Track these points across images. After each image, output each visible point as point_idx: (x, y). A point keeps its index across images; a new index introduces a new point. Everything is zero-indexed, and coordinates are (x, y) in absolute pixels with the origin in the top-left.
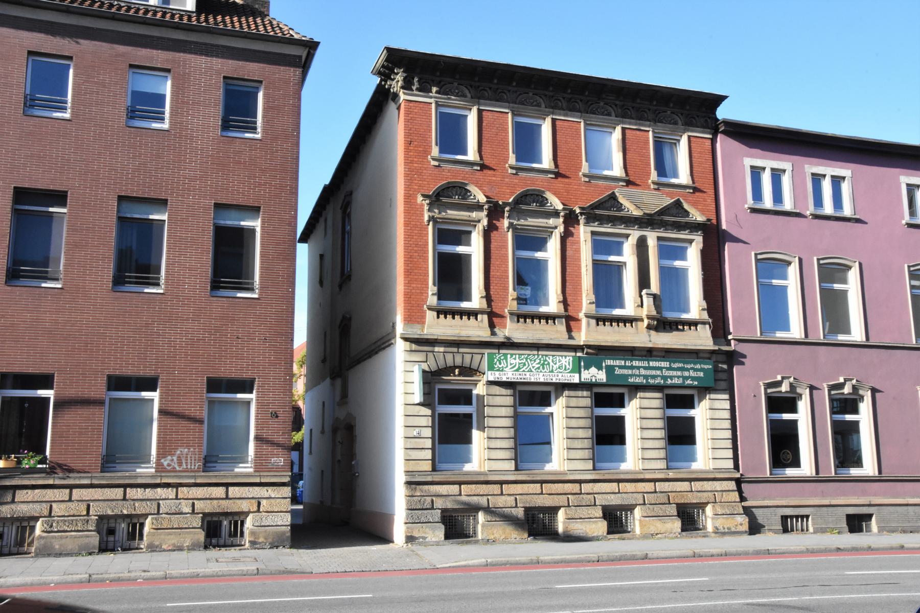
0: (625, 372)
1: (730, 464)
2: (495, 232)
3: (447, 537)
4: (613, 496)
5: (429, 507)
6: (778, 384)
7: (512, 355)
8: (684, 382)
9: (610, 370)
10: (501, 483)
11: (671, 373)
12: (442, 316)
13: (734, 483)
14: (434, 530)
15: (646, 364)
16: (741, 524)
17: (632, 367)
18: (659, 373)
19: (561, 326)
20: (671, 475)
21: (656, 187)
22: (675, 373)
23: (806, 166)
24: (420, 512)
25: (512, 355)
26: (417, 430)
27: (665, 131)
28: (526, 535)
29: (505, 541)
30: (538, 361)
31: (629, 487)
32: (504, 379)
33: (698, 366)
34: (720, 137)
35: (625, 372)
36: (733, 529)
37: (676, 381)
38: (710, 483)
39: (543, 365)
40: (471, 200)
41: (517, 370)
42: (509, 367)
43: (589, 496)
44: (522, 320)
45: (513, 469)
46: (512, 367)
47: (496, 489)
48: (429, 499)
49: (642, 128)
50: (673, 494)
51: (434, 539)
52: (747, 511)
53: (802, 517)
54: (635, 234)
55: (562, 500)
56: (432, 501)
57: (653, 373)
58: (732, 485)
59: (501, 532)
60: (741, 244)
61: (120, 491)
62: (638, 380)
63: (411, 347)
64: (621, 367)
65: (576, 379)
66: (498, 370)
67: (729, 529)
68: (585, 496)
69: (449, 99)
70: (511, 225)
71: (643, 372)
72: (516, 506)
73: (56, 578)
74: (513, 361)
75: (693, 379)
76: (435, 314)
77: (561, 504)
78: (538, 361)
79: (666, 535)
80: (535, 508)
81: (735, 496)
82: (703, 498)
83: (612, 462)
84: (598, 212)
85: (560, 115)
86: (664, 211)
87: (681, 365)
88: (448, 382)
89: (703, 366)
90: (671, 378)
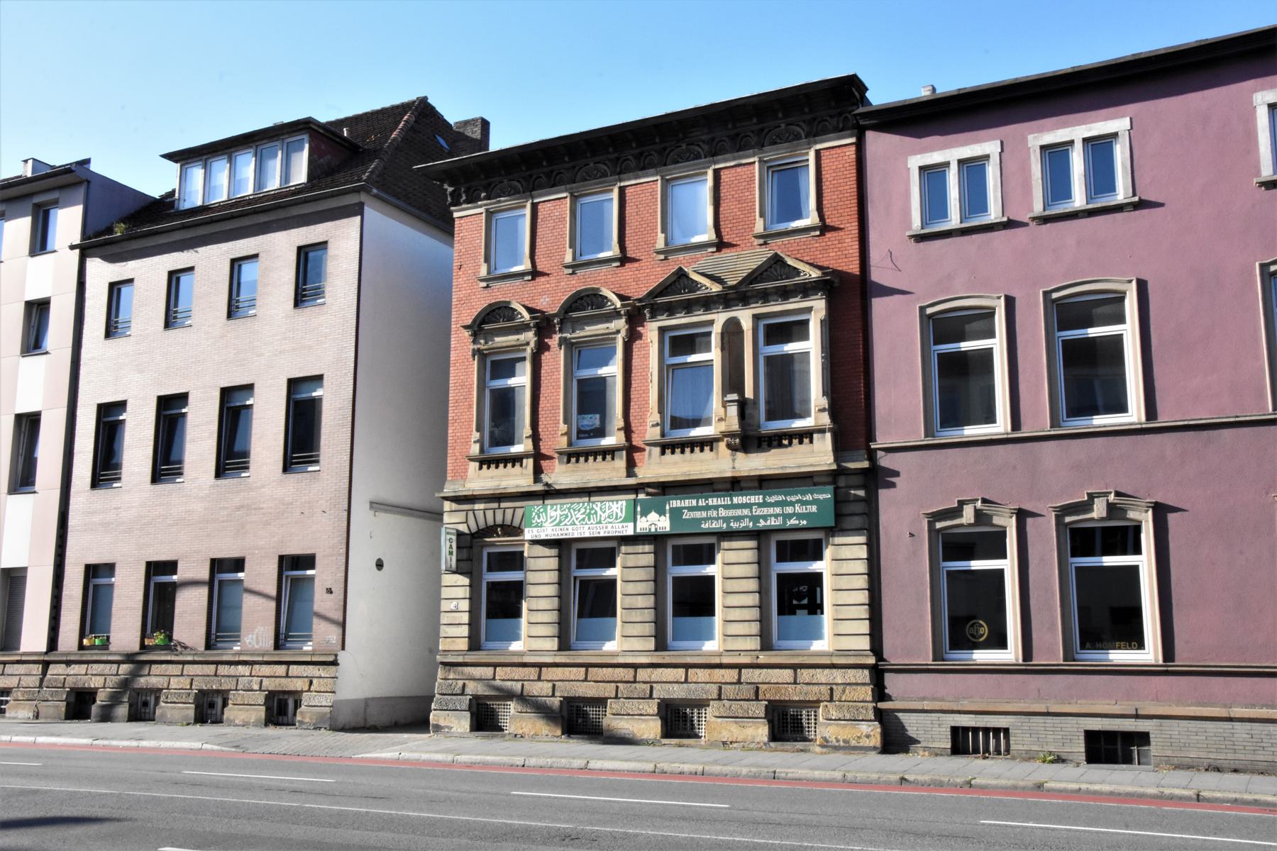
0: (698, 514)
1: (864, 644)
3: (775, 736)
4: (676, 686)
6: (956, 512)
8: (785, 522)
9: (676, 514)
10: (540, 666)
11: (765, 511)
13: (866, 672)
14: (459, 719)
15: (727, 501)
16: (868, 736)
17: (707, 508)
18: (746, 512)
19: (620, 463)
20: (763, 658)
21: (761, 241)
22: (771, 511)
23: (1030, 137)
25: (552, 505)
26: (455, 602)
27: (776, 154)
28: (559, 732)
31: (702, 675)
32: (543, 537)
33: (809, 497)
34: (870, 136)
35: (698, 514)
36: (853, 743)
37: (773, 523)
38: (827, 671)
40: (609, 308)
41: (558, 525)
43: (644, 686)
44: (573, 460)
45: (556, 648)
46: (550, 521)
47: (532, 673)
48: (460, 683)
52: (880, 716)
53: (997, 731)
54: (720, 318)
55: (608, 690)
56: (464, 685)
57: (739, 512)
58: (864, 675)
61: (681, 671)
62: (716, 526)
64: (691, 509)
65: (629, 531)
67: (844, 741)
70: (563, 341)
71: (723, 513)
72: (553, 695)
73: (745, 771)
74: (553, 514)
76: (477, 464)
77: (607, 695)
79: (746, 746)
80: (584, 698)
81: (867, 693)
82: (812, 693)
84: (660, 300)
85: (629, 179)
86: (755, 276)
87: (780, 498)
88: (492, 544)
89: (816, 496)
90: (765, 518)
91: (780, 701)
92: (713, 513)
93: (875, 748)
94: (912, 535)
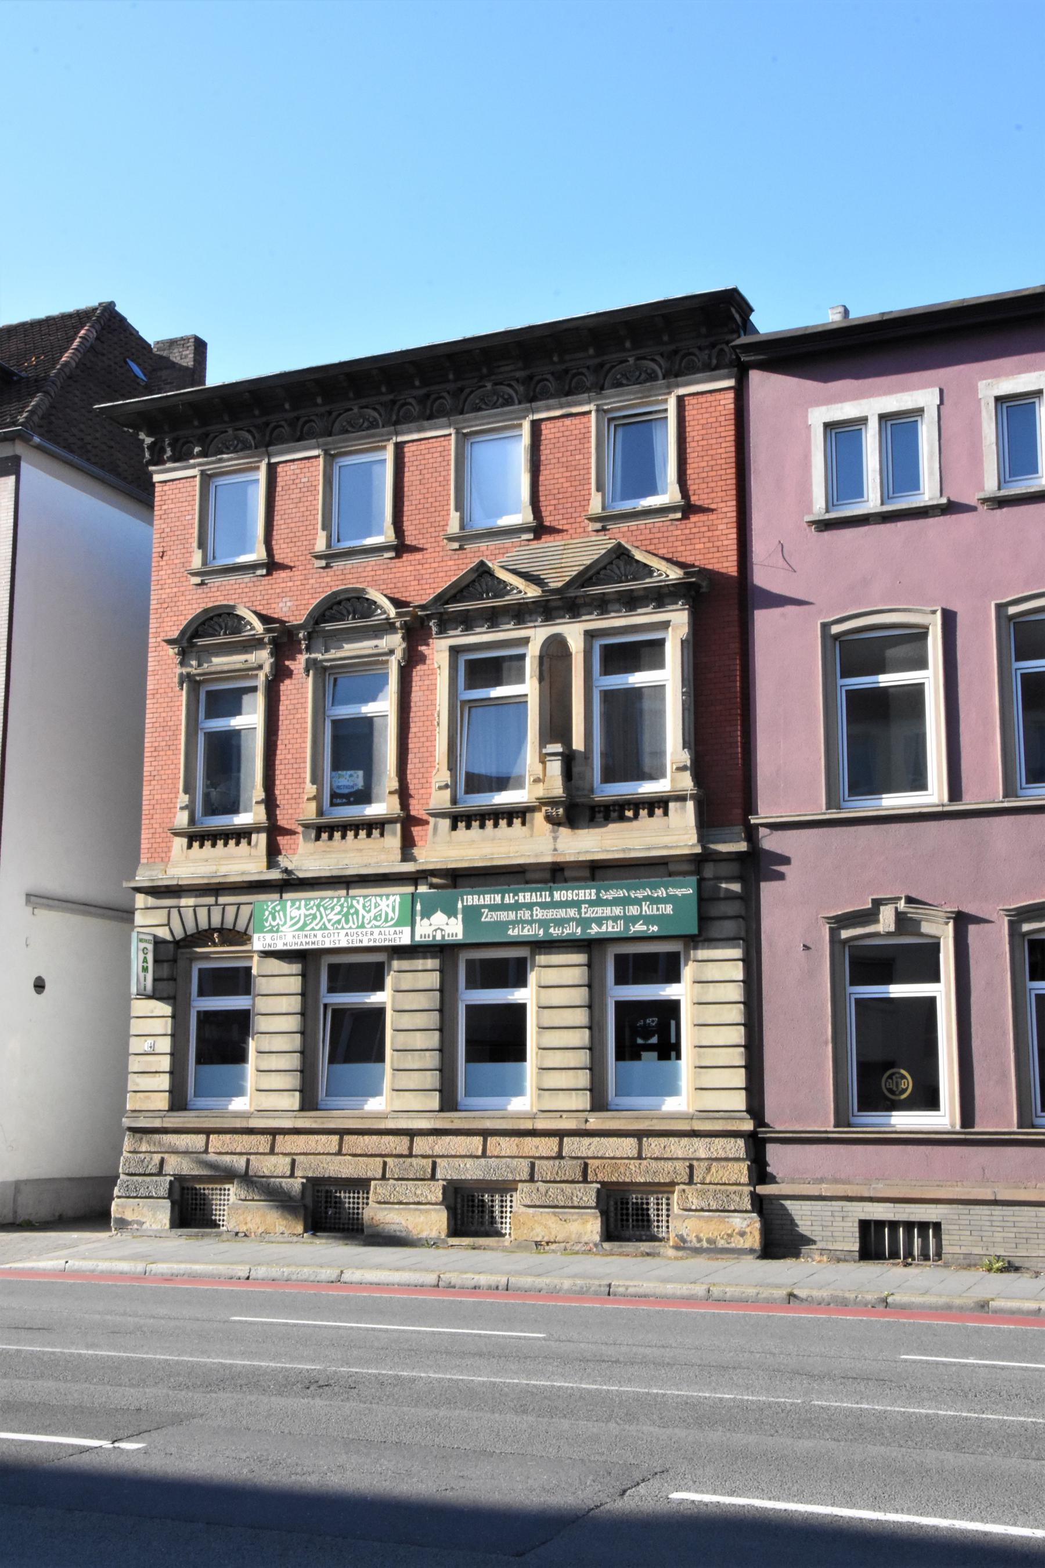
0: (503, 916)
1: (738, 1101)
2: (287, 682)
3: (609, 1235)
4: (469, 1162)
5: (154, 1171)
6: (870, 916)
7: (293, 901)
9: (472, 915)
10: (274, 1132)
11: (600, 911)
12: (461, 825)
13: (741, 1142)
14: (154, 1209)
15: (546, 897)
16: (742, 1234)
17: (517, 907)
18: (572, 913)
19: (393, 841)
20: (595, 1122)
21: (598, 526)
22: (607, 911)
23: (982, 385)
24: (140, 1179)
25: (293, 901)
26: (150, 1041)
27: (622, 401)
28: (300, 1229)
29: (264, 1236)
30: (338, 909)
31: (506, 1145)
32: (280, 947)
33: (661, 893)
34: (755, 377)
35: (503, 916)
36: (721, 1243)
37: (610, 928)
38: (685, 1141)
39: (346, 916)
40: (378, 618)
41: (302, 929)
42: (289, 923)
43: (424, 1162)
44: (325, 836)
45: (297, 1107)
46: (292, 923)
47: (262, 1143)
48: (157, 1158)
49: (575, 410)
50: (597, 1162)
51: (154, 1227)
52: (760, 1204)
53: (923, 1226)
54: (538, 635)
57: (561, 913)
58: (738, 1147)
59: (258, 1220)
60: (790, 609)
61: (478, 1141)
62: (528, 932)
63: (145, 902)
64: (493, 908)
65: (404, 938)
66: (271, 931)
67: (709, 1241)
68: (493, 1162)
69: (221, 460)
70: (311, 665)
71: (539, 913)
72: (292, 1175)
73: (567, 1284)
74: (295, 913)
75: (648, 920)
76: (185, 841)
77: (370, 1175)
78: (338, 909)
79: (569, 1248)
80: (336, 1179)
81: (741, 1171)
82: (663, 1173)
83: (628, 1095)
84: (453, 608)
85: (410, 432)
86: (588, 576)
87: (621, 893)
88: (206, 957)
89: (672, 891)
90: (599, 921)
91: (618, 1183)
92: (525, 914)
93: (752, 1251)
94: (806, 948)
